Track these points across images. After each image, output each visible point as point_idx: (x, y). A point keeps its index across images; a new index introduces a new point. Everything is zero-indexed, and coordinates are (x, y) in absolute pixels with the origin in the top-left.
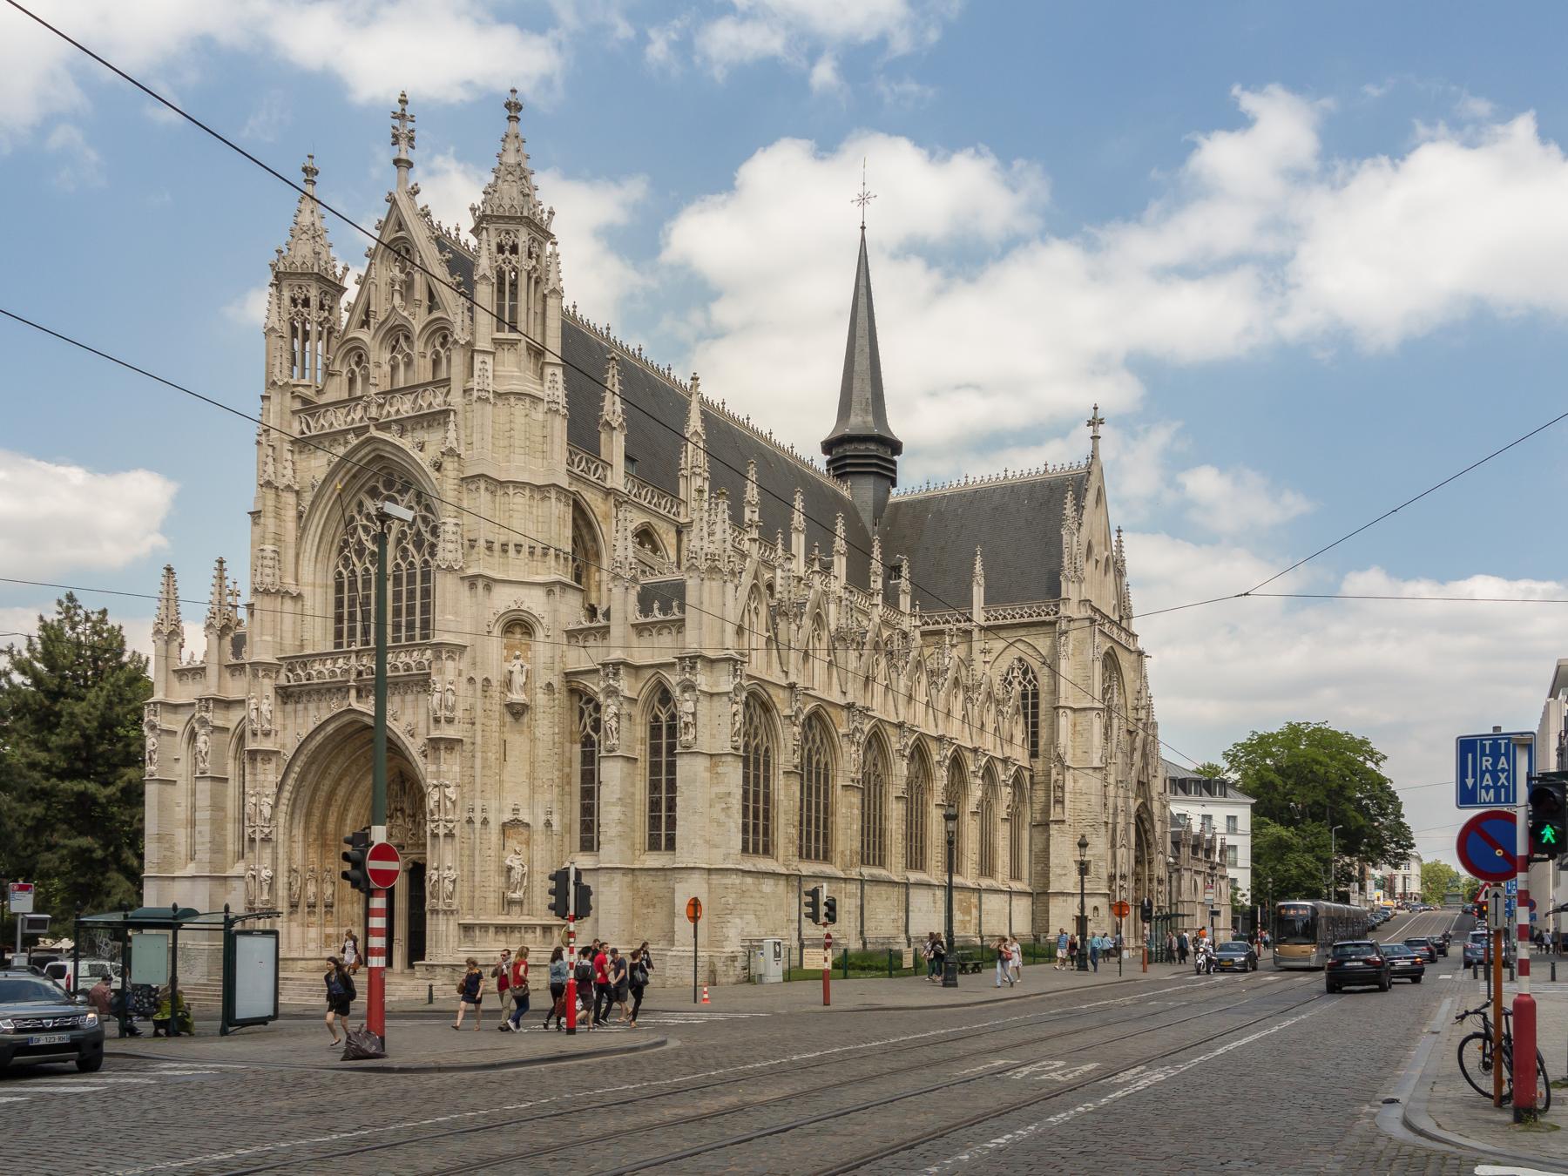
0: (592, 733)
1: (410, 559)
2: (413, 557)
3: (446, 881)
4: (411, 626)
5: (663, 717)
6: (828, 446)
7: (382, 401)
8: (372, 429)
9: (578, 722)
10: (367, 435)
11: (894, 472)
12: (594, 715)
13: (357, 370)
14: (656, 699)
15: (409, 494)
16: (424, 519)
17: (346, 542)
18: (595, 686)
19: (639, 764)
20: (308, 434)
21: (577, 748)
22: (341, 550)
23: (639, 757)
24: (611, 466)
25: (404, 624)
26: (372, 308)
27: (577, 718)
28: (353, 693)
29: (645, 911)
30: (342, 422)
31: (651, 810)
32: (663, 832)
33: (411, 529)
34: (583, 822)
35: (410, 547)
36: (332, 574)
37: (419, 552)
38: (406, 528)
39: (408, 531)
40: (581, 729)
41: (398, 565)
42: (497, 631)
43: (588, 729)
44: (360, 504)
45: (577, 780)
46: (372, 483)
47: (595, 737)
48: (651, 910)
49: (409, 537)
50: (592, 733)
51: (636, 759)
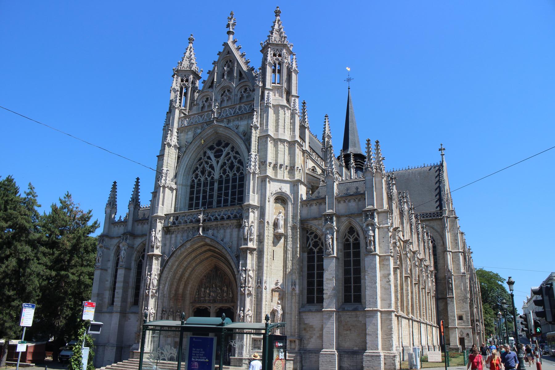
2: (229, 172)
3: (248, 316)
5: (351, 240)
14: (347, 231)
15: (228, 147)
16: (235, 158)
17: (197, 168)
21: (306, 255)
22: (194, 171)
27: (305, 241)
28: (201, 229)
29: (345, 332)
31: (345, 283)
34: (308, 290)
36: (190, 181)
40: (307, 246)
41: (221, 177)
42: (272, 199)
43: (311, 246)
44: (205, 153)
45: (305, 269)
46: (211, 144)
48: (348, 332)
50: (313, 248)
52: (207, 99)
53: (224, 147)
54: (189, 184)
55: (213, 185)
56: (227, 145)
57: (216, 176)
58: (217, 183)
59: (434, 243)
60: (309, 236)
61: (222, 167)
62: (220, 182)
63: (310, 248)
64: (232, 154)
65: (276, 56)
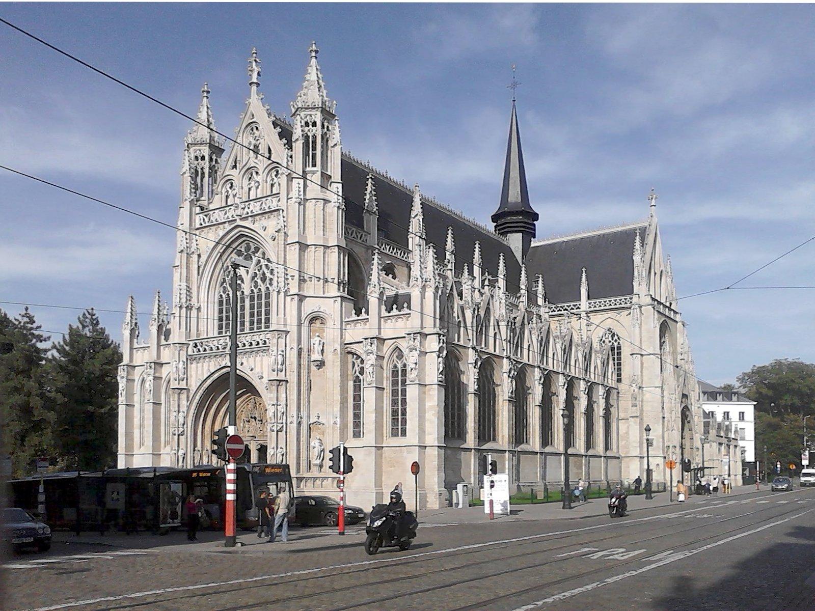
0: (359, 375)
1: (259, 287)
4: (259, 322)
5: (399, 366)
6: (495, 218)
7: (244, 206)
8: (238, 220)
9: (351, 369)
10: (236, 224)
11: (535, 230)
12: (361, 366)
13: (230, 191)
18: (359, 349)
19: (385, 391)
20: (204, 225)
23: (385, 387)
24: (370, 234)
25: (255, 321)
26: (238, 159)
30: (222, 218)
32: (400, 427)
33: (259, 271)
35: (259, 281)
37: (263, 283)
38: (257, 271)
39: (258, 273)
41: (252, 291)
42: (307, 323)
47: (361, 377)
49: (258, 275)
51: (384, 388)
52: (232, 184)
53: (254, 253)
54: (216, 300)
55: (244, 302)
56: (257, 249)
57: (247, 292)
58: (248, 299)
59: (619, 343)
60: (355, 361)
61: (253, 278)
62: (252, 299)
63: (355, 375)
64: (263, 262)
65: (308, 126)
